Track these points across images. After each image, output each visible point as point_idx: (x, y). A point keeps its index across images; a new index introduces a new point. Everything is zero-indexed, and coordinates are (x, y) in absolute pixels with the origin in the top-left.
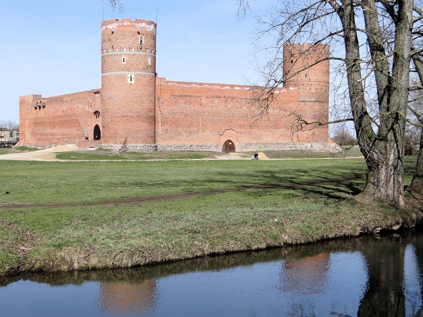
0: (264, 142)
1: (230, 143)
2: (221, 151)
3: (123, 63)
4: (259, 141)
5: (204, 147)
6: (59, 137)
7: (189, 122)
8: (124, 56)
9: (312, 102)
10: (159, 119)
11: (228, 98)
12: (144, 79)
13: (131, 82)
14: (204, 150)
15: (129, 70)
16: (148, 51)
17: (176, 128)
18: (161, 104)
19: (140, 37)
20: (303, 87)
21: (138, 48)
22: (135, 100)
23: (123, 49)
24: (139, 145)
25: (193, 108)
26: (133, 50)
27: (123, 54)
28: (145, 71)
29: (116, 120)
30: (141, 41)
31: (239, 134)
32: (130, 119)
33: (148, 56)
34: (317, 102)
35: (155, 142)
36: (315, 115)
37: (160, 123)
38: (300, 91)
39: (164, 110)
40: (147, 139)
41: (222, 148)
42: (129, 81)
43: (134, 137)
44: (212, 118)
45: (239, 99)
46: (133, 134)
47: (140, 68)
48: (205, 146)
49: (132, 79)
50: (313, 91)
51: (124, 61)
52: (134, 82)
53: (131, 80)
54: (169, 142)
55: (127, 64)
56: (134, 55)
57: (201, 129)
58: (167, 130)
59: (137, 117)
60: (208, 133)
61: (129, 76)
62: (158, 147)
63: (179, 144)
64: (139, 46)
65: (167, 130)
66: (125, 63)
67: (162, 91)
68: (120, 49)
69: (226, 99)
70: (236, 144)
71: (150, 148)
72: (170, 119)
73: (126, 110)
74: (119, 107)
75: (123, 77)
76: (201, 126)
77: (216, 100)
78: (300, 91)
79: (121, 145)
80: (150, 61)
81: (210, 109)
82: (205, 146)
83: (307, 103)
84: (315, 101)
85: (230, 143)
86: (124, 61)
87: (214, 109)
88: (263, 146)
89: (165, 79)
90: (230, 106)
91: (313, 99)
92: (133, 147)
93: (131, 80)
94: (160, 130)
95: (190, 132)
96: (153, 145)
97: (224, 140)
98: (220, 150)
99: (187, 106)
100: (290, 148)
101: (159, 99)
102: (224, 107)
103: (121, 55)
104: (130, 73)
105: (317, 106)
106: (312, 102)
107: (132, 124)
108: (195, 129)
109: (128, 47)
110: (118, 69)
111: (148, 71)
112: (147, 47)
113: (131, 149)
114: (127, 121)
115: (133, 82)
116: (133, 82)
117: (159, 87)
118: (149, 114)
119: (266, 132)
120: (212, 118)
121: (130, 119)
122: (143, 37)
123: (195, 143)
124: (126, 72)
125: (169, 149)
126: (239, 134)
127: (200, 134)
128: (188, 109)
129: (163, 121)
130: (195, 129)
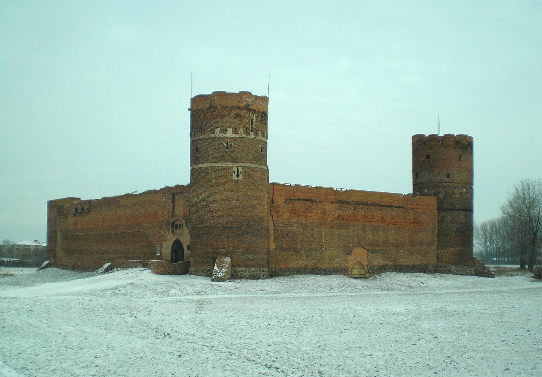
6: (112, 256)
10: (272, 231)
11: (357, 203)
15: (234, 161)
32: (236, 231)
34: (462, 210)
37: (272, 237)
42: (234, 177)
59: (247, 228)
61: (235, 169)
67: (275, 192)
74: (220, 213)
76: (324, 242)
93: (238, 176)
115: (241, 177)
121: (236, 231)
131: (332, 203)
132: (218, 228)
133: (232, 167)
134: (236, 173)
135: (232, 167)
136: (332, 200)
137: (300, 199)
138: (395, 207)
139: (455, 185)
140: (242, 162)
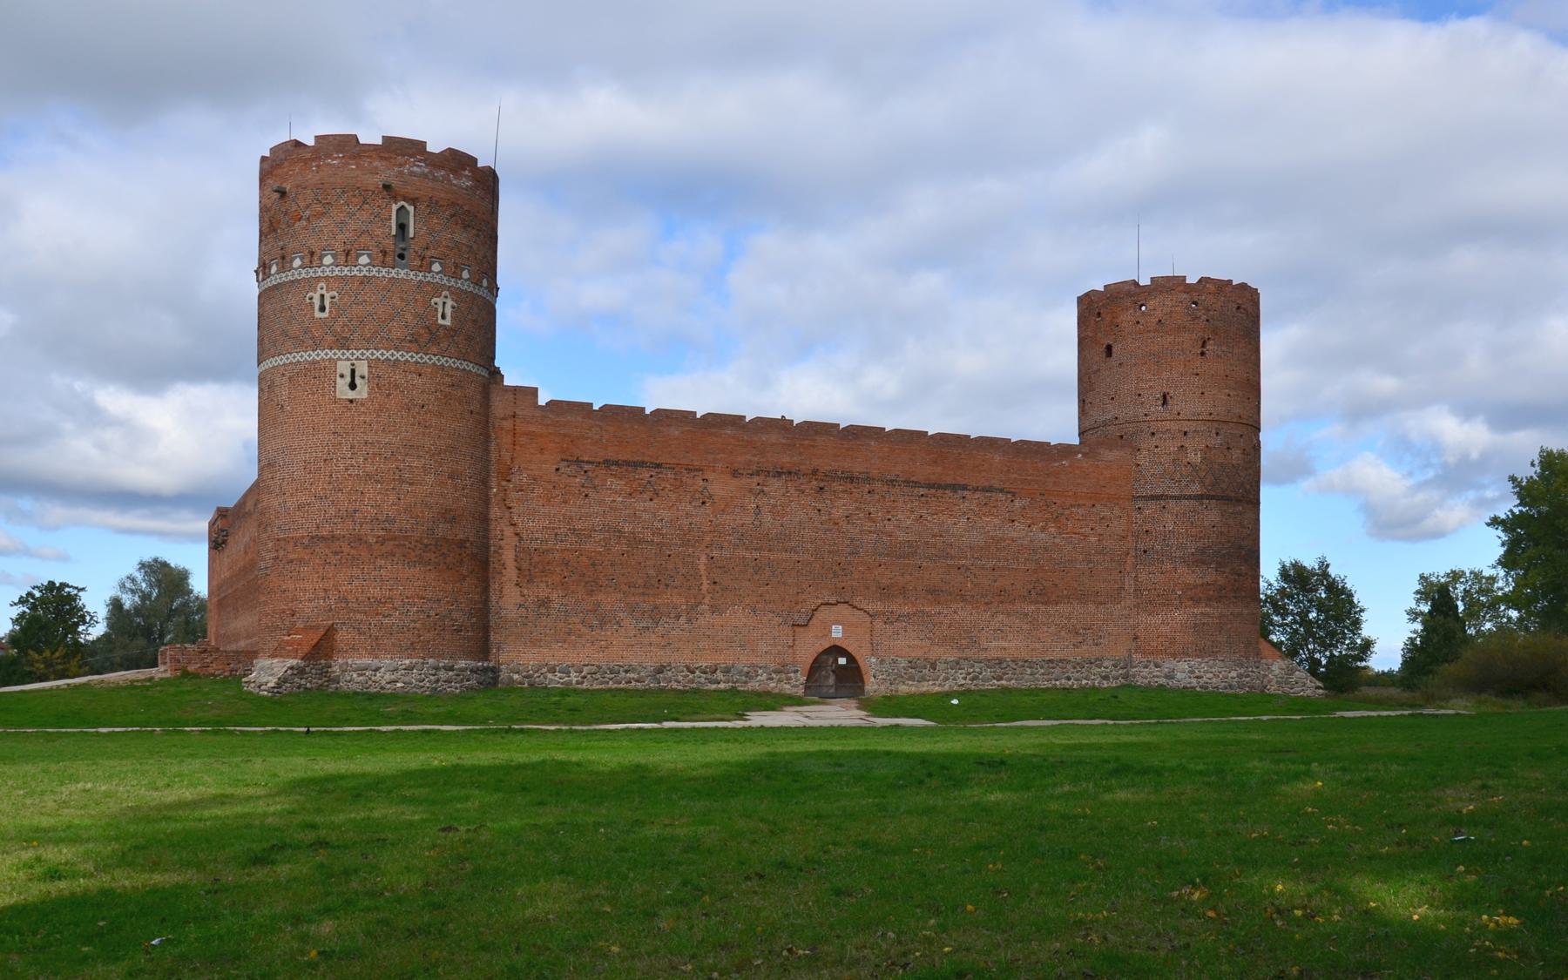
0: (994, 654)
1: (842, 661)
2: (800, 691)
3: (318, 314)
4: (968, 653)
5: (719, 675)
7: (652, 572)
8: (322, 288)
9: (1189, 498)
10: (509, 556)
11: (831, 476)
12: (418, 381)
13: (351, 395)
14: (722, 686)
15: (343, 343)
16: (436, 267)
17: (590, 594)
18: (513, 495)
19: (395, 207)
20: (1154, 441)
21: (384, 253)
22: (370, 468)
23: (321, 258)
24: (387, 662)
25: (666, 514)
26: (364, 260)
27: (319, 279)
28: (422, 349)
29: (291, 556)
30: (402, 227)
31: (879, 624)
32: (346, 549)
33: (437, 290)
34: (1213, 497)
35: (483, 648)
36: (1203, 551)
37: (511, 573)
38: (1143, 459)
39: (530, 517)
40: (428, 636)
41: (803, 679)
42: (343, 391)
43: (364, 628)
44: (756, 555)
45: (878, 485)
46: (358, 616)
47: (397, 333)
48: (727, 671)
49: (358, 381)
50: (1195, 458)
51: (322, 309)
52: (365, 395)
53: (353, 386)
54: (558, 655)
55: (334, 319)
56: (365, 281)
57: (706, 600)
58: (544, 603)
60: (737, 617)
61: (344, 367)
62: (503, 675)
63: (601, 659)
64: (389, 244)
65: (544, 603)
66: (326, 315)
67: (523, 440)
68: (307, 261)
69: (823, 481)
70: (868, 663)
71: (443, 675)
72: (557, 555)
73: (332, 511)
74: (303, 499)
75: (320, 374)
76: (705, 587)
77: (774, 485)
78: (1143, 459)
79: (293, 662)
80: (448, 311)
81: (748, 520)
82: (727, 671)
83: (1172, 503)
84: (1200, 497)
85: (842, 661)
86: (322, 309)
87: (767, 518)
88: (988, 673)
89: (533, 392)
90: (838, 513)
91: (1196, 489)
92: (361, 670)
93: (353, 386)
94: (509, 598)
95: (656, 614)
96: (462, 664)
97: (808, 648)
98: (795, 683)
99: (640, 506)
100: (1106, 678)
101: (506, 475)
102: (813, 514)
103: (311, 283)
104: (348, 354)
105: (1212, 515)
106: (1189, 498)
107: (356, 571)
108: (676, 600)
109: (339, 247)
110: (300, 344)
111: (435, 350)
112: (429, 253)
113: (353, 681)
114: (334, 560)
116: (362, 392)
117: (507, 424)
118: (442, 529)
119: (1001, 617)
120: (756, 555)
121: (346, 549)
122: (411, 209)
123: (681, 659)
124: (331, 354)
125: (555, 680)
126: (879, 624)
127: (702, 621)
128: (645, 516)
129: (525, 565)
130: (676, 600)
131: (735, 474)
132: (296, 542)
133: (333, 362)
134: (348, 379)
135: (333, 362)
136: (736, 466)
137: (617, 463)
138: (976, 490)
139: (1186, 427)
140: (368, 342)
